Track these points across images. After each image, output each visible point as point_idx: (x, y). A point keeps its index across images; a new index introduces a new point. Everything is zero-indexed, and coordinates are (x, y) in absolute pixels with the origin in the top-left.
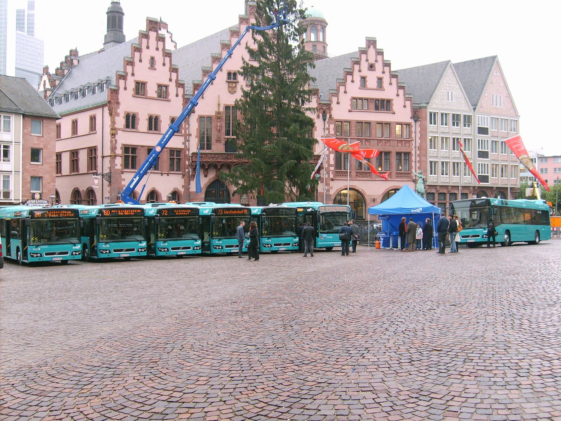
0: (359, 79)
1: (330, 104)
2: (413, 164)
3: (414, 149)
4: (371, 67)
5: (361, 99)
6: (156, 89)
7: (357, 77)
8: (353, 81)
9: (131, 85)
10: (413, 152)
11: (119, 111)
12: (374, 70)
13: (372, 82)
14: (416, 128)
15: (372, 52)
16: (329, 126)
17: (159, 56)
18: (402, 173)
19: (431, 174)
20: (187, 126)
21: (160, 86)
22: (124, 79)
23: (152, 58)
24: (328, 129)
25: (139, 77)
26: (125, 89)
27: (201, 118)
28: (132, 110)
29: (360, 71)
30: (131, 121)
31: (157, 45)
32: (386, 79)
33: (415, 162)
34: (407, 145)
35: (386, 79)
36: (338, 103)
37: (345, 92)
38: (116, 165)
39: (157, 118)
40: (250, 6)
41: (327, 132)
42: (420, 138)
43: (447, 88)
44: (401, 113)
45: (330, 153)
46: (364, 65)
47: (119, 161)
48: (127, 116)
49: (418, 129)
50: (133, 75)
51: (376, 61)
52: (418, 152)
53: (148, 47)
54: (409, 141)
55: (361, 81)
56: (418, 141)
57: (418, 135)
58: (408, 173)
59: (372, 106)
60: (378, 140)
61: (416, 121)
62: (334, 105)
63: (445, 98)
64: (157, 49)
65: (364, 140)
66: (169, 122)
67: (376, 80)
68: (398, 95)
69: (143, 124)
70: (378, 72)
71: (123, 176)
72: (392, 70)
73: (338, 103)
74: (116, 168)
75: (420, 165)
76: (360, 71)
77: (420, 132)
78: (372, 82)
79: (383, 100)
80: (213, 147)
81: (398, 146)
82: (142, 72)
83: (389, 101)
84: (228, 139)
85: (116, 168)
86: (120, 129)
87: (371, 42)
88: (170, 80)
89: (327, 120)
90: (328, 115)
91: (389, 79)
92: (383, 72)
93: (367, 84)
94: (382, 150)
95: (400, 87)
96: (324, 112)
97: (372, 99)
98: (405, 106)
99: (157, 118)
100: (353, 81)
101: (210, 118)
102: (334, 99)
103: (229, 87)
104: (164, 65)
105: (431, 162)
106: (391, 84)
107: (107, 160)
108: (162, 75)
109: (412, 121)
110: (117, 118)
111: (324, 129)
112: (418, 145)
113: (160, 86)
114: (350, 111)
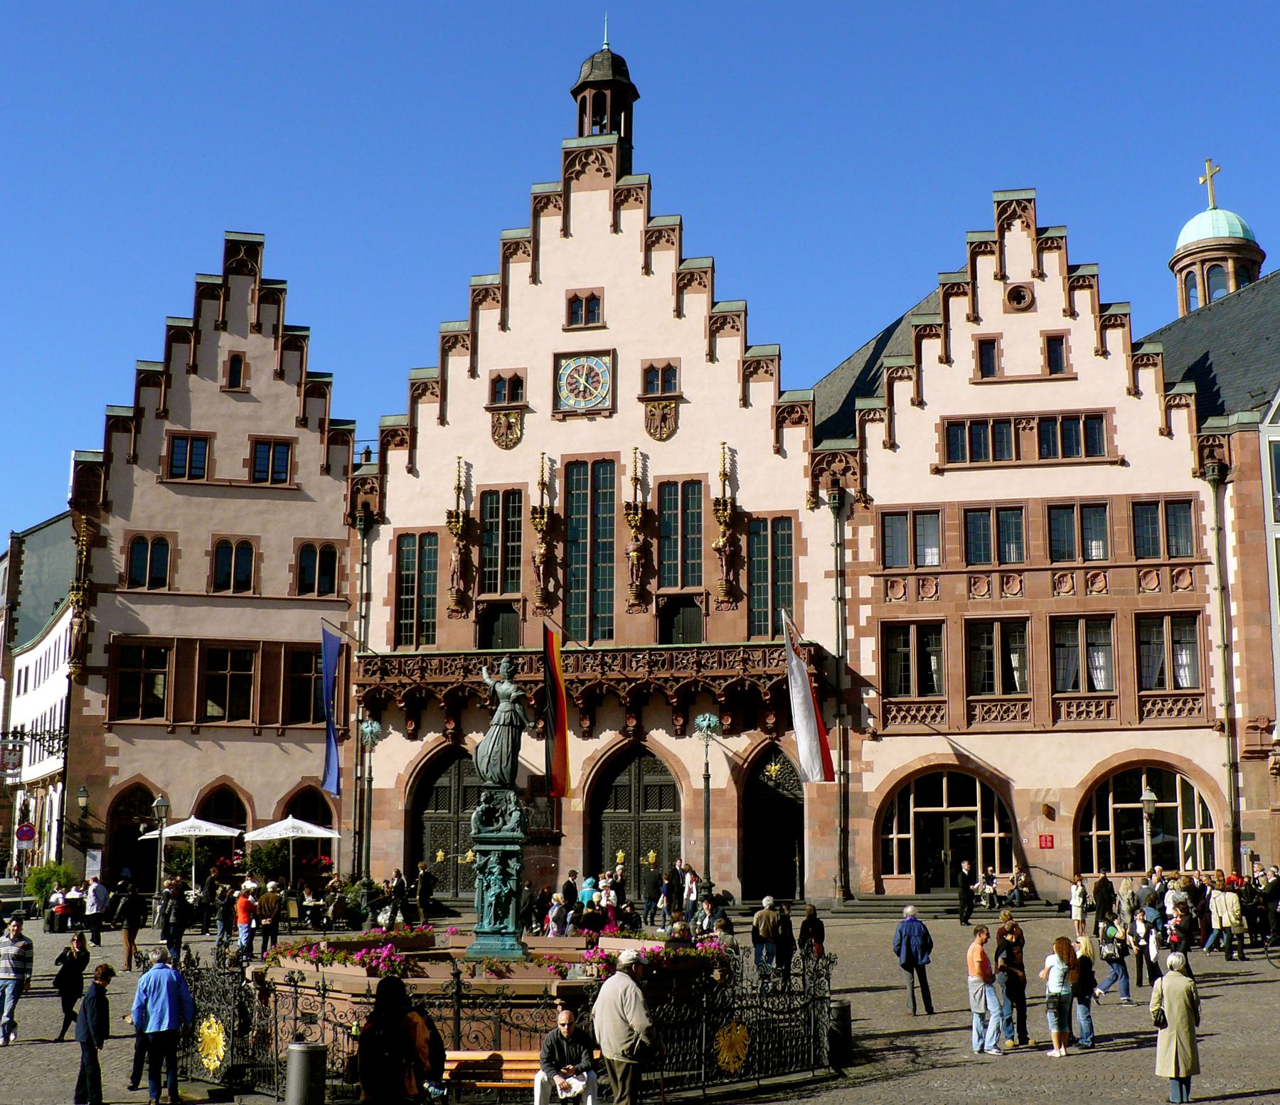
0: (971, 346)
2: (1216, 658)
3: (1215, 597)
4: (1019, 298)
5: (979, 423)
8: (946, 359)
10: (1213, 609)
12: (1031, 306)
15: (1019, 241)
16: (855, 533)
17: (261, 352)
18: (1164, 698)
20: (358, 567)
21: (260, 444)
23: (236, 362)
24: (854, 544)
27: (402, 538)
29: (975, 318)
30: (151, 561)
34: (1185, 581)
36: (891, 444)
37: (919, 402)
39: (246, 547)
40: (567, 154)
45: (861, 633)
46: (991, 294)
48: (136, 543)
58: (1196, 697)
59: (1030, 441)
61: (1219, 484)
66: (291, 558)
67: (1040, 343)
79: (1070, 419)
80: (440, 634)
83: (1095, 419)
84: (491, 604)
86: (107, 588)
88: (303, 422)
92: (1071, 312)
95: (1138, 361)
96: (835, 483)
97: (1028, 417)
98: (1167, 432)
99: (246, 547)
100: (946, 359)
101: (429, 536)
102: (875, 433)
103: (495, 427)
113: (260, 444)
114: (938, 471)
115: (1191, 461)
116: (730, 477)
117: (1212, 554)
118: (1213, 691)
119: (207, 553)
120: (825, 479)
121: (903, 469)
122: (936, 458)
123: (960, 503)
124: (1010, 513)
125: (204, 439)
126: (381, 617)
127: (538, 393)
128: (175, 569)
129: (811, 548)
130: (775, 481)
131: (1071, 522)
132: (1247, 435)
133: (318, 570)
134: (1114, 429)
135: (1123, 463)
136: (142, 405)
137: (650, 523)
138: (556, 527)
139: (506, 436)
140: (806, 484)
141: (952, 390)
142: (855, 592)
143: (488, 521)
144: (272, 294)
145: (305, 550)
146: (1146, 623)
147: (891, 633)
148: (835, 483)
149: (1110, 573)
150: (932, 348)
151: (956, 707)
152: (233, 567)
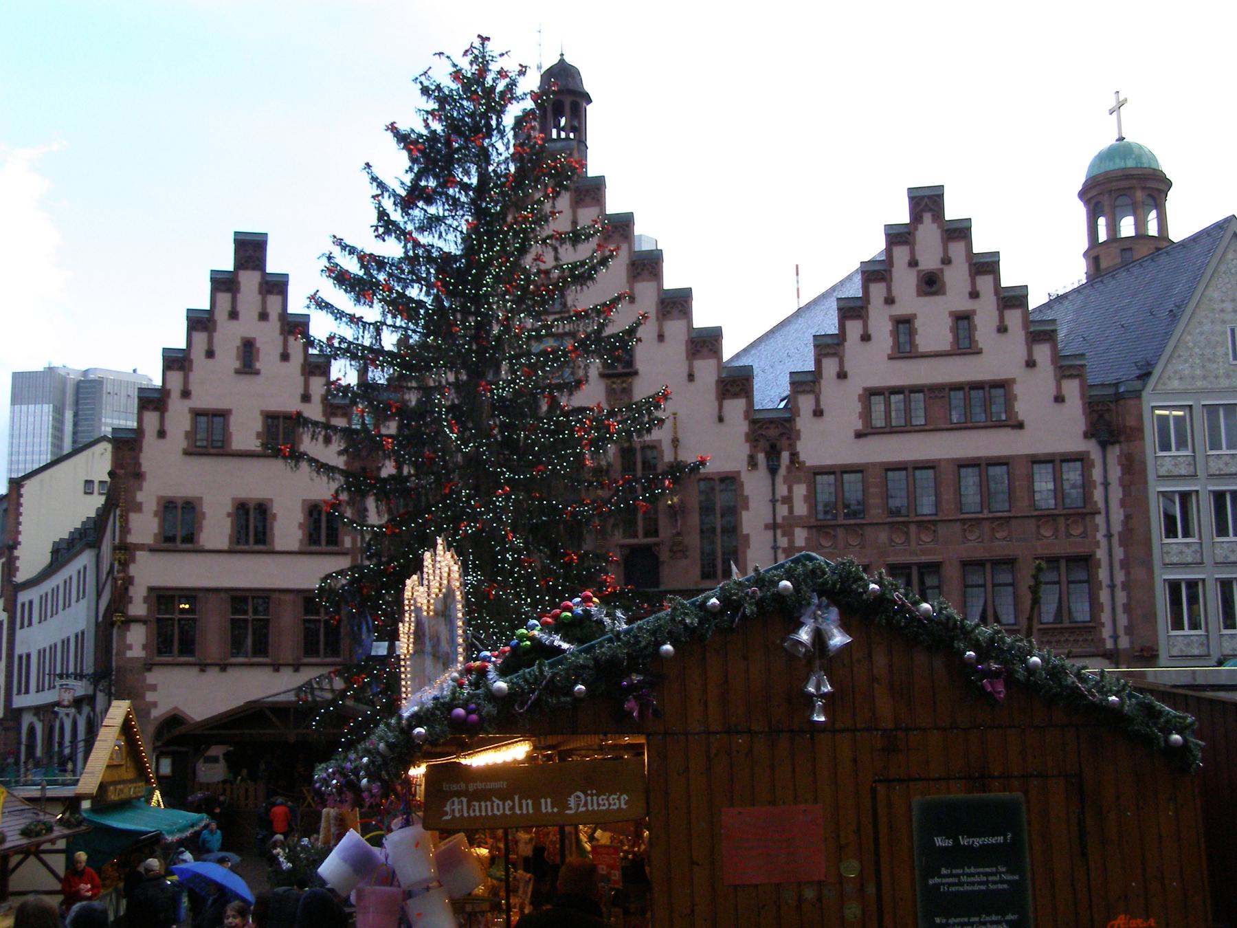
0: (888, 326)
1: (791, 420)
2: (1104, 596)
4: (931, 284)
6: (258, 426)
7: (880, 322)
8: (866, 338)
9: (179, 417)
10: (1101, 554)
11: (140, 497)
13: (934, 330)
14: (1107, 468)
15: (928, 234)
16: (790, 490)
17: (268, 337)
19: (1178, 625)
21: (271, 418)
22: (156, 409)
24: (788, 500)
25: (204, 399)
26: (162, 434)
28: (181, 489)
29: (890, 301)
31: (264, 303)
32: (986, 315)
33: (1112, 587)
34: (1077, 530)
35: (986, 315)
36: (818, 413)
37: (842, 375)
38: (130, 647)
41: (783, 510)
42: (1123, 503)
43: (1227, 317)
44: (1050, 422)
46: (905, 281)
49: (1115, 472)
50: (186, 394)
51: (946, 261)
52: (1119, 553)
53: (234, 315)
54: (1083, 516)
55: (895, 334)
56: (1117, 515)
57: (1116, 493)
60: (963, 521)
61: (1104, 445)
62: (805, 423)
63: (1220, 351)
64: (264, 316)
65: (913, 528)
66: (299, 516)
67: (948, 322)
68: (1031, 364)
69: (216, 528)
70: (956, 296)
72: (1006, 282)
73: (818, 413)
74: (129, 654)
75: (1129, 597)
76: (890, 301)
77: (1121, 480)
78: (934, 330)
81: (1039, 536)
82: (215, 384)
85: (129, 654)
86: (141, 547)
87: (927, 202)
89: (782, 471)
90: (785, 456)
91: (996, 314)
92: (974, 295)
93: (919, 340)
94: (980, 554)
96: (773, 447)
98: (1059, 399)
100: (866, 338)
102: (806, 403)
104: (285, 357)
105: (1174, 587)
106: (1002, 329)
108: (279, 387)
109: (1092, 447)
110: (134, 518)
111: (774, 501)
112: (1117, 528)
113: (271, 418)
114: (859, 435)
115: (1080, 425)
117: (1101, 505)
118: (1103, 625)
119: (229, 515)
120: (762, 443)
122: (859, 425)
123: (881, 464)
125: (223, 415)
128: (200, 529)
129: (752, 504)
132: (1132, 402)
134: (1015, 397)
135: (1020, 426)
136: (168, 386)
140: (744, 450)
141: (872, 364)
142: (791, 541)
144: (277, 286)
148: (773, 447)
149: (1014, 523)
152: (252, 526)
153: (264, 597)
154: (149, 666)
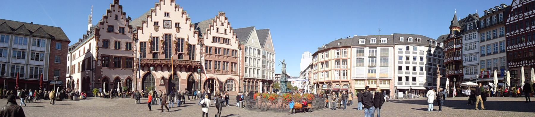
5: (217, 38)
13: (222, 30)
27: (141, 43)
36: (207, 38)
39: (119, 42)
47: (99, 63)
48: (104, 41)
71: (102, 70)
78: (222, 30)
79: (226, 39)
83: (229, 40)
99: (119, 42)
101: (145, 43)
102: (205, 37)
107: (94, 62)
116: (188, 39)
121: (208, 42)
124: (219, 48)
126: (138, 53)
127: (161, 24)
130: (194, 40)
131: (226, 50)
133: (129, 46)
137: (178, 44)
138: (165, 43)
139: (157, 30)
141: (214, 33)
143: (154, 41)
145: (127, 43)
146: (232, 63)
147: (206, 61)
150: (212, 28)
151: (213, 71)
153: (119, 58)
154: (101, 68)
